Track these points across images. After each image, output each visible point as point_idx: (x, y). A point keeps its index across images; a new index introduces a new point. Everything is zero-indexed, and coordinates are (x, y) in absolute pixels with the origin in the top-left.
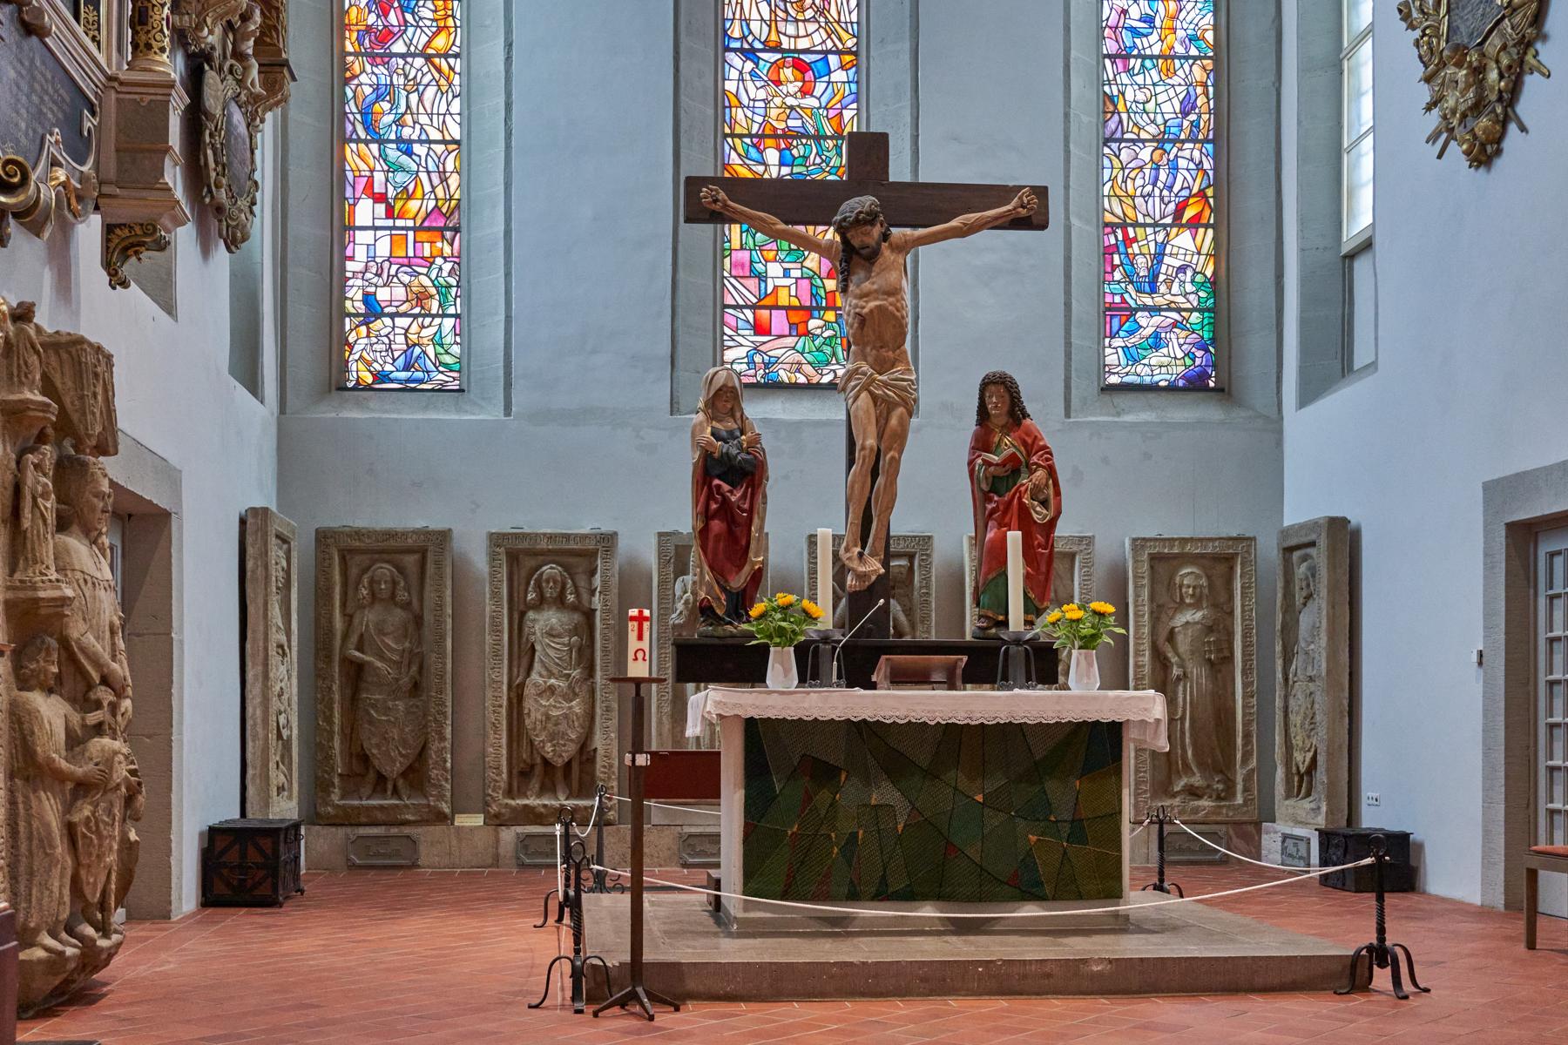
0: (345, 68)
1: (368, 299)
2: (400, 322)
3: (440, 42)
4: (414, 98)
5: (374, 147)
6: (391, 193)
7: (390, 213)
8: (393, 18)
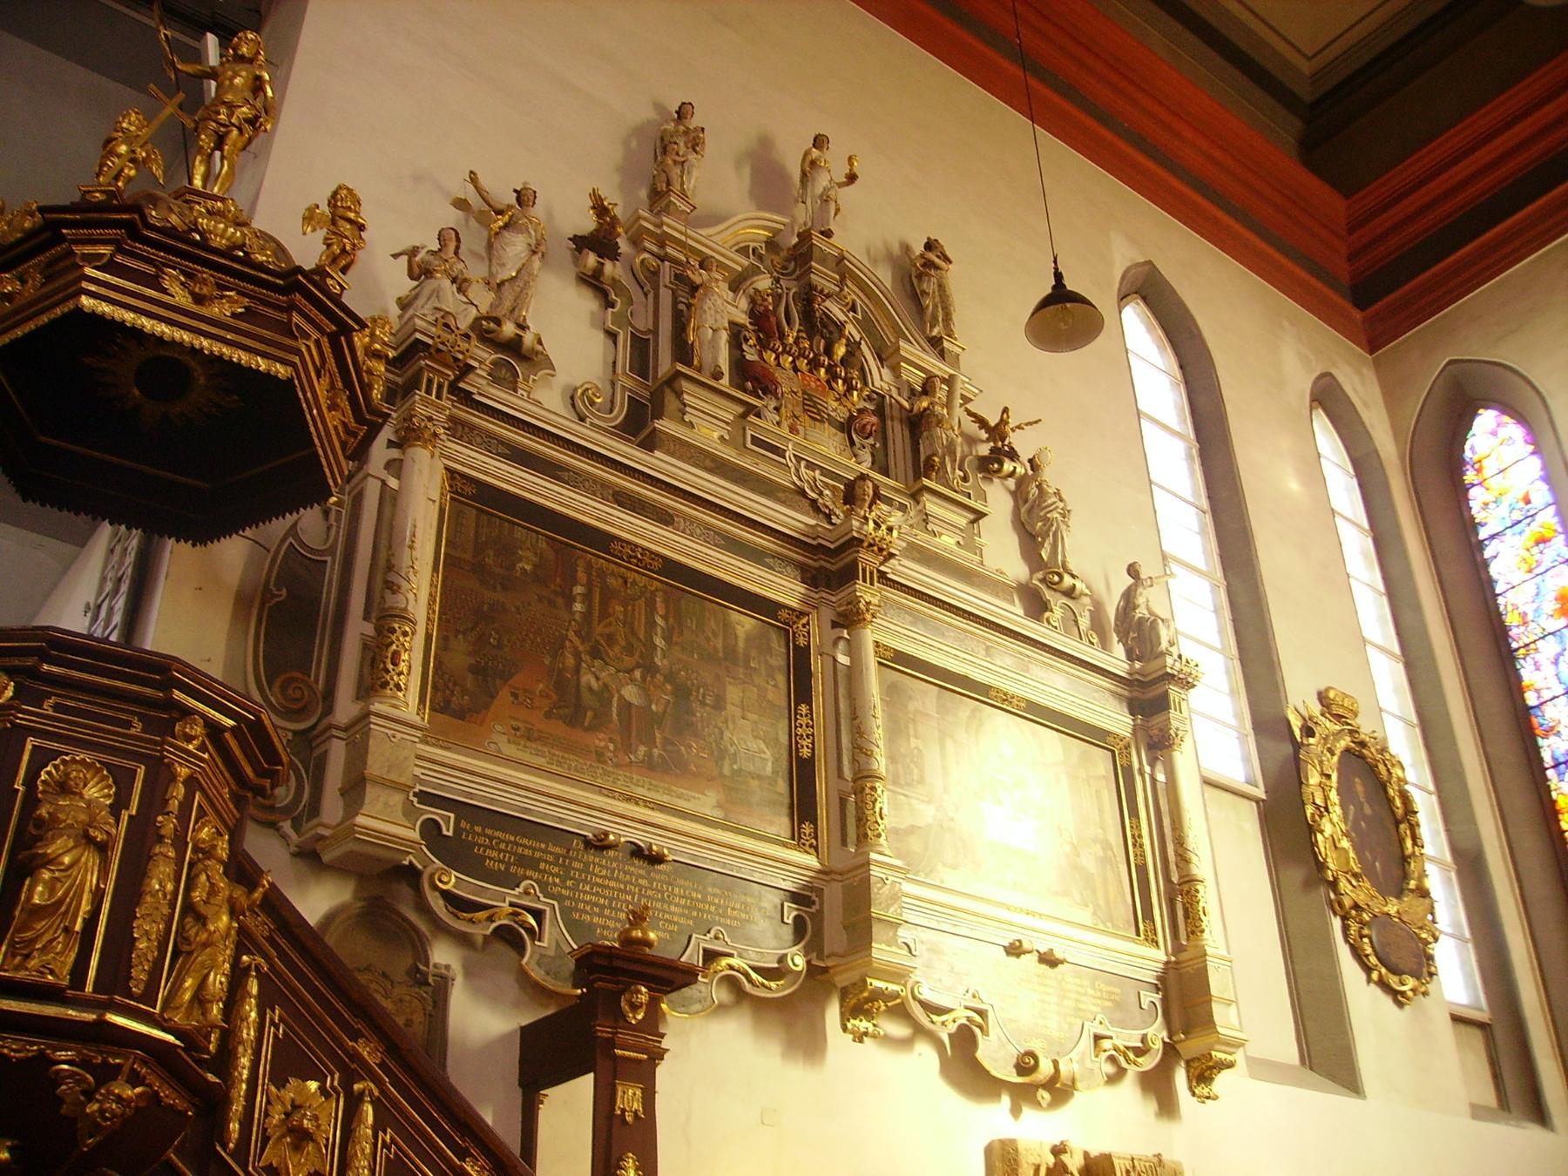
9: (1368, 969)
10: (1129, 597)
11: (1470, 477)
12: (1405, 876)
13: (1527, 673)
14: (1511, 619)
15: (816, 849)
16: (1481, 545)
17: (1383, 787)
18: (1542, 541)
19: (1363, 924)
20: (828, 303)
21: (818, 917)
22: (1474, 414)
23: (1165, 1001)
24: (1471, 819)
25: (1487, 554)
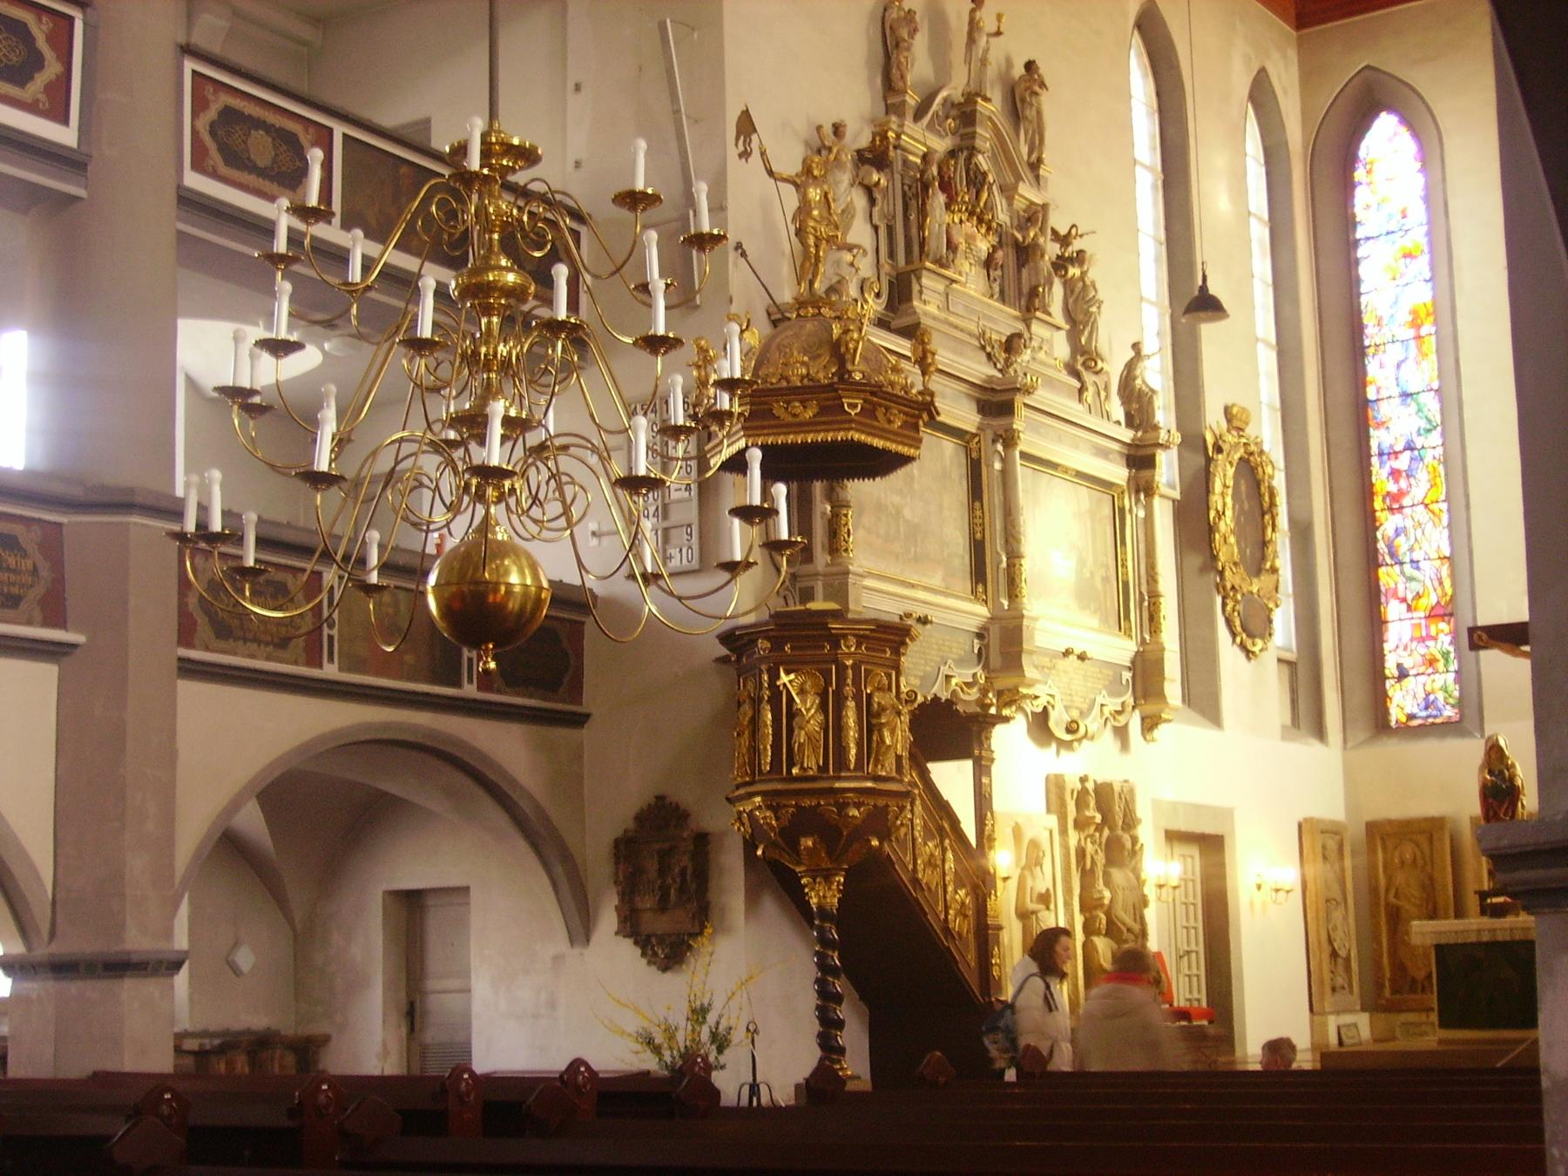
0: (1374, 519)
1: (1399, 666)
2: (1422, 679)
3: (1432, 496)
4: (1419, 531)
5: (1397, 568)
6: (1410, 597)
7: (1409, 608)
8: (1403, 483)
9: (1234, 635)
10: (1130, 367)
11: (1359, 175)
12: (1263, 558)
13: (1372, 366)
14: (1368, 319)
15: (986, 602)
16: (1356, 243)
17: (1258, 484)
18: (1408, 256)
19: (1237, 602)
20: (980, 157)
21: (987, 646)
22: (1376, 115)
23: (1133, 677)
24: (1307, 495)
25: (1361, 253)
